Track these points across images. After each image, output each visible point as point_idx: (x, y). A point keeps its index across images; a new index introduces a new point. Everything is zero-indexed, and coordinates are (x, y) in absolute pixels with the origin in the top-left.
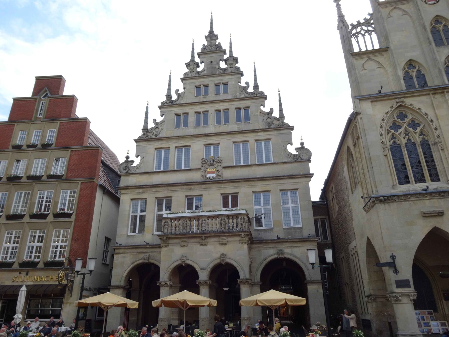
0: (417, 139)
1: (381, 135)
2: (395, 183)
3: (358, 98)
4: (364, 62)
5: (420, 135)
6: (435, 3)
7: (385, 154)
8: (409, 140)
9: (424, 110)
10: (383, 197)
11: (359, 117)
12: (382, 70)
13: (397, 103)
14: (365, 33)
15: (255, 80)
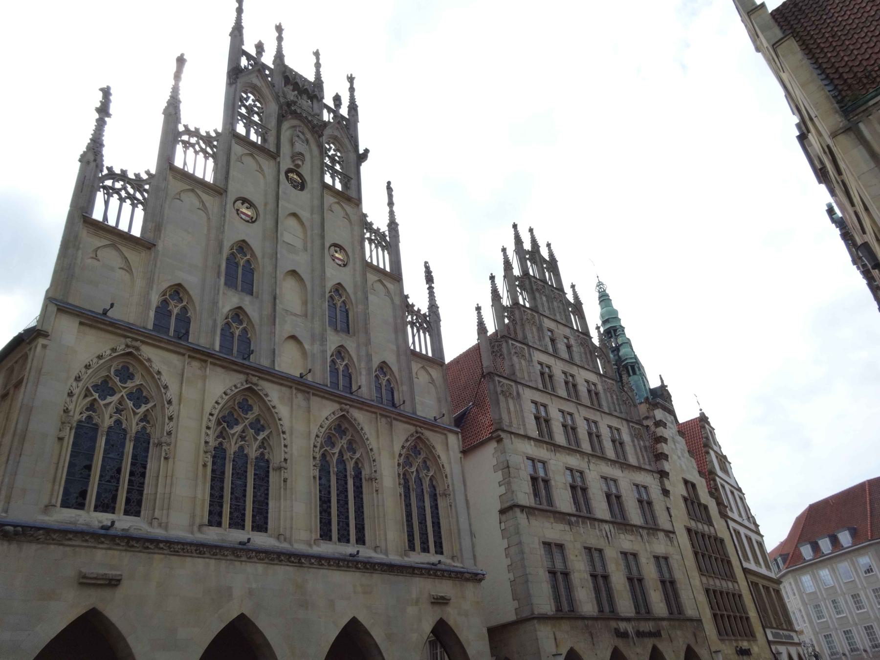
0: (133, 426)
1: (70, 394)
2: (53, 501)
3: (58, 302)
4: (100, 244)
5: (141, 420)
6: (248, 221)
7: (61, 436)
8: (118, 422)
9: (167, 378)
10: (15, 526)
11: (42, 341)
12: (126, 277)
13: (127, 346)
14: (126, 198)
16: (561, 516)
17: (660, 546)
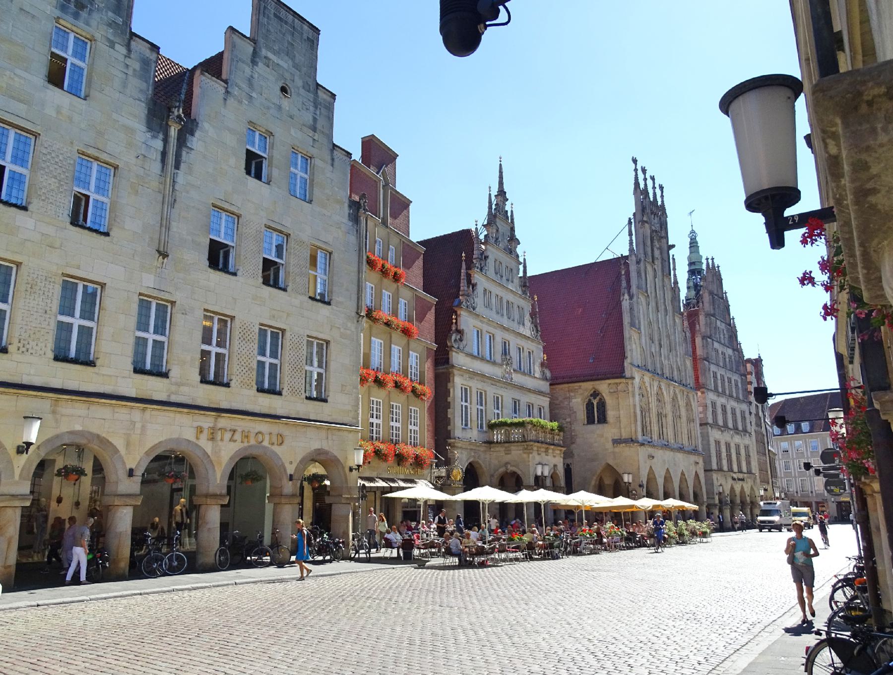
9: (649, 389)
16: (719, 428)
17: (747, 441)
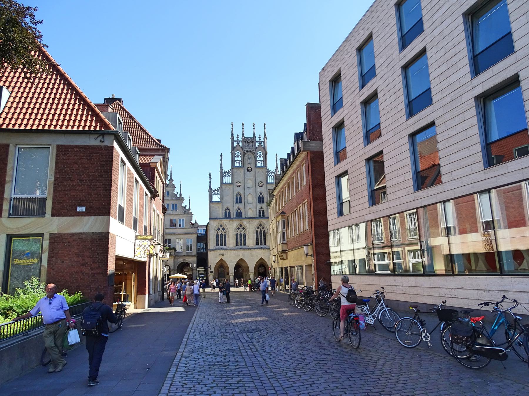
0: (223, 234)
3: (211, 219)
15: (181, 192)
